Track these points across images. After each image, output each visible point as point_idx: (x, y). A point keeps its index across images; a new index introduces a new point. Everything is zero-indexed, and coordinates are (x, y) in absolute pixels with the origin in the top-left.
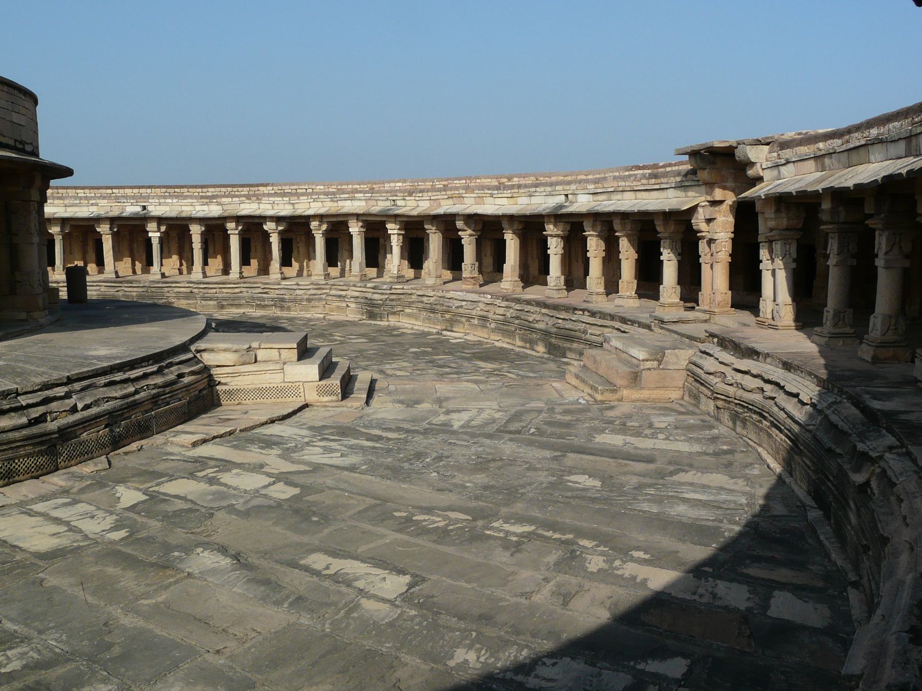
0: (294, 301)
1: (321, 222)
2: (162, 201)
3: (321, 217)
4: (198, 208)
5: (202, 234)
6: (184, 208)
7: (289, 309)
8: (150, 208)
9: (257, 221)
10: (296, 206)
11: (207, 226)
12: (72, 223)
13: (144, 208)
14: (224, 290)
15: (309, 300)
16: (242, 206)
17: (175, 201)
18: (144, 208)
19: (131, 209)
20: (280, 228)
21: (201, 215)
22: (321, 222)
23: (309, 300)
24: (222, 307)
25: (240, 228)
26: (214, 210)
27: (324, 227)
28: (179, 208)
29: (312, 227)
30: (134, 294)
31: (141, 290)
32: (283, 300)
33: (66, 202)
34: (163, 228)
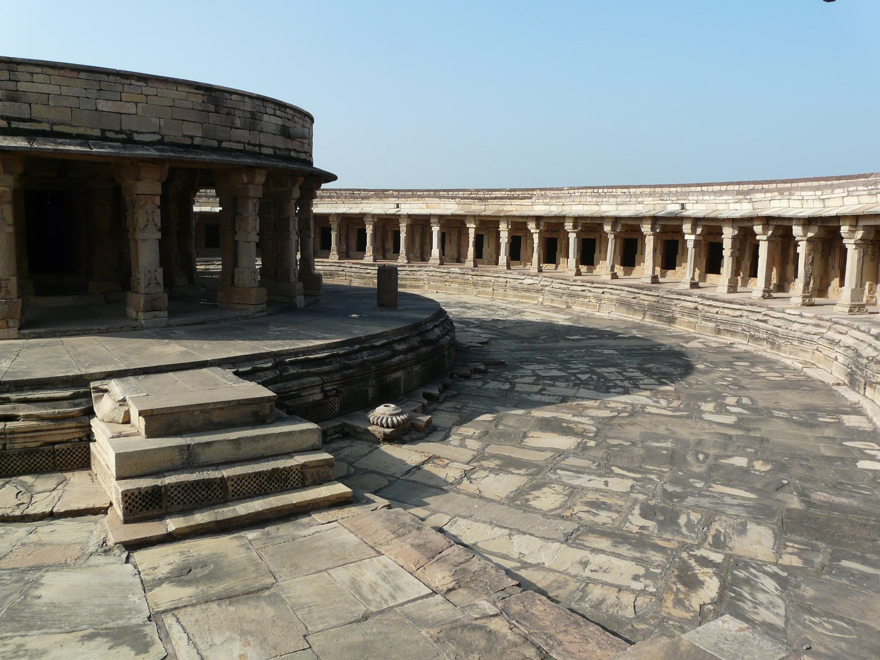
0: (786, 337)
1: (854, 227)
2: (700, 198)
3: (855, 219)
4: (733, 206)
5: (734, 238)
6: (720, 207)
7: (779, 348)
8: (688, 206)
9: (521, 220)
10: (828, 203)
11: (740, 229)
12: (623, 222)
13: (683, 206)
14: (726, 311)
15: (801, 340)
16: (774, 203)
17: (712, 198)
18: (683, 206)
19: (672, 208)
20: (810, 235)
21: (737, 215)
22: (854, 227)
23: (801, 340)
24: (718, 332)
25: (770, 233)
26: (743, 209)
27: (859, 234)
28: (714, 207)
29: (684, 231)
30: (646, 303)
31: (654, 299)
32: (776, 334)
33: (619, 200)
34: (699, 231)
